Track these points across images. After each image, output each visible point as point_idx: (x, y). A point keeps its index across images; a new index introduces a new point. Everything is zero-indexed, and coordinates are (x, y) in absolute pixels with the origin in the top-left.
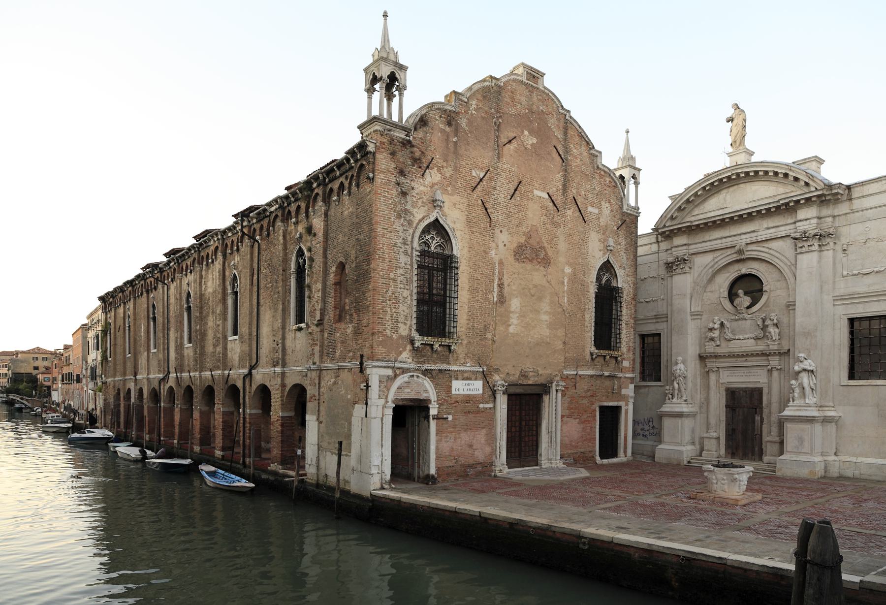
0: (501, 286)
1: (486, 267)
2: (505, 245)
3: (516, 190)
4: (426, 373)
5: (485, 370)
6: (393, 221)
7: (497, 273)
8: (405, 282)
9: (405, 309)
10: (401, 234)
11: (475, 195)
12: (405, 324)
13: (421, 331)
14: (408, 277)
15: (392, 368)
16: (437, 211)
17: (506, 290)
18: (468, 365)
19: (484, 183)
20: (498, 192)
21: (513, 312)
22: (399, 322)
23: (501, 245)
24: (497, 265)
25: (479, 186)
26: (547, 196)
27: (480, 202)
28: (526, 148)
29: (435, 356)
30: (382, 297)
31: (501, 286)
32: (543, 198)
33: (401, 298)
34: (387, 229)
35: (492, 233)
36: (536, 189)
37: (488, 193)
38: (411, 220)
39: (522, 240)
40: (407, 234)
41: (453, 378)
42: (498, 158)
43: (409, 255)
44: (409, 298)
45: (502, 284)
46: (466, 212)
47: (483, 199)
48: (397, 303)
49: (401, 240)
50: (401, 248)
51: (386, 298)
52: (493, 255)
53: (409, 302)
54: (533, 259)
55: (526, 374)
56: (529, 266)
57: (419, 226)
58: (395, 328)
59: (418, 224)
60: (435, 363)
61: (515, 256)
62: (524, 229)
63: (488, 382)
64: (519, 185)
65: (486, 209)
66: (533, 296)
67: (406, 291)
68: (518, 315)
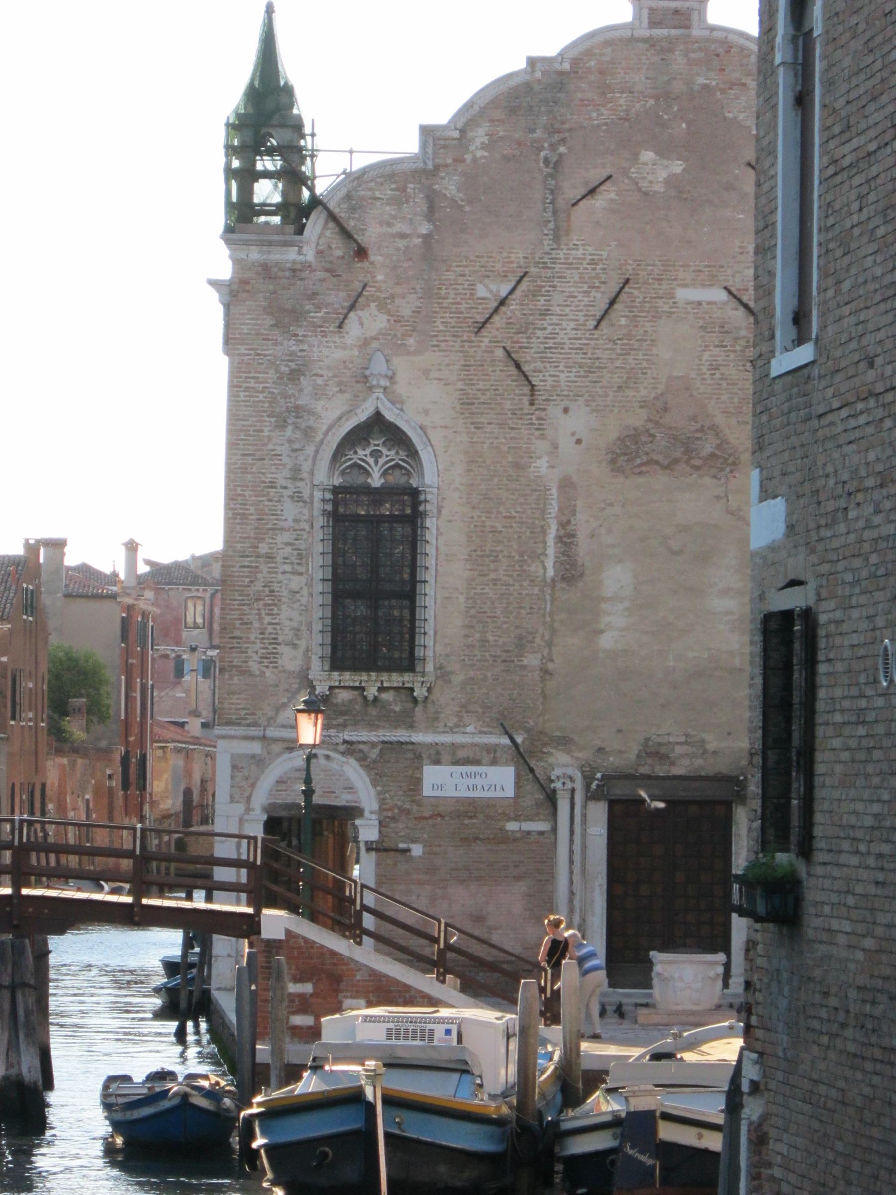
0: (567, 539)
1: (522, 500)
2: (579, 441)
3: (612, 303)
4: (351, 749)
5: (519, 740)
6: (269, 436)
7: (553, 509)
8: (294, 559)
9: (295, 615)
10: (285, 459)
11: (486, 340)
12: (295, 646)
13: (337, 663)
14: (302, 547)
15: (264, 738)
16: (375, 396)
17: (583, 547)
18: (469, 730)
19: (513, 305)
20: (555, 319)
21: (610, 599)
22: (279, 644)
23: (566, 445)
24: (554, 492)
25: (496, 318)
26: (723, 296)
27: (500, 353)
28: (646, 194)
29: (373, 711)
30: (240, 595)
31: (567, 539)
32: (709, 303)
33: (285, 593)
34: (254, 455)
35: (539, 419)
36: (685, 286)
37: (525, 328)
38: (310, 427)
39: (638, 419)
40: (301, 458)
41: (425, 762)
42: (557, 238)
43: (304, 502)
44: (305, 592)
45: (572, 535)
46: (460, 385)
47: (508, 345)
48: (275, 605)
49: (286, 472)
50: (285, 488)
51: (248, 595)
52: (543, 470)
53: (304, 601)
54: (676, 461)
55: (663, 750)
56: (660, 480)
57: (329, 437)
58: (270, 658)
59: (326, 433)
60: (372, 726)
61: (613, 461)
62: (644, 392)
63: (532, 770)
64: (622, 288)
65: (518, 366)
66: (675, 553)
67: (296, 578)
68: (626, 604)
